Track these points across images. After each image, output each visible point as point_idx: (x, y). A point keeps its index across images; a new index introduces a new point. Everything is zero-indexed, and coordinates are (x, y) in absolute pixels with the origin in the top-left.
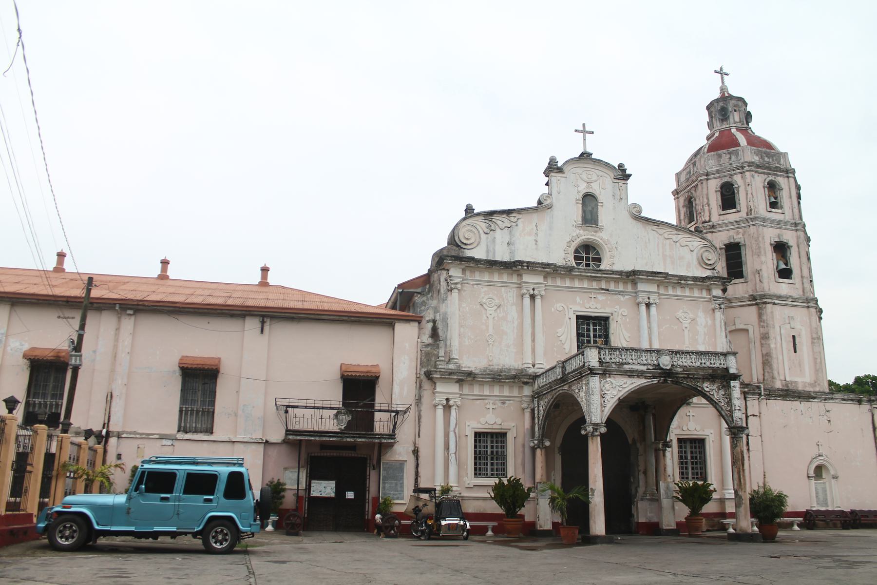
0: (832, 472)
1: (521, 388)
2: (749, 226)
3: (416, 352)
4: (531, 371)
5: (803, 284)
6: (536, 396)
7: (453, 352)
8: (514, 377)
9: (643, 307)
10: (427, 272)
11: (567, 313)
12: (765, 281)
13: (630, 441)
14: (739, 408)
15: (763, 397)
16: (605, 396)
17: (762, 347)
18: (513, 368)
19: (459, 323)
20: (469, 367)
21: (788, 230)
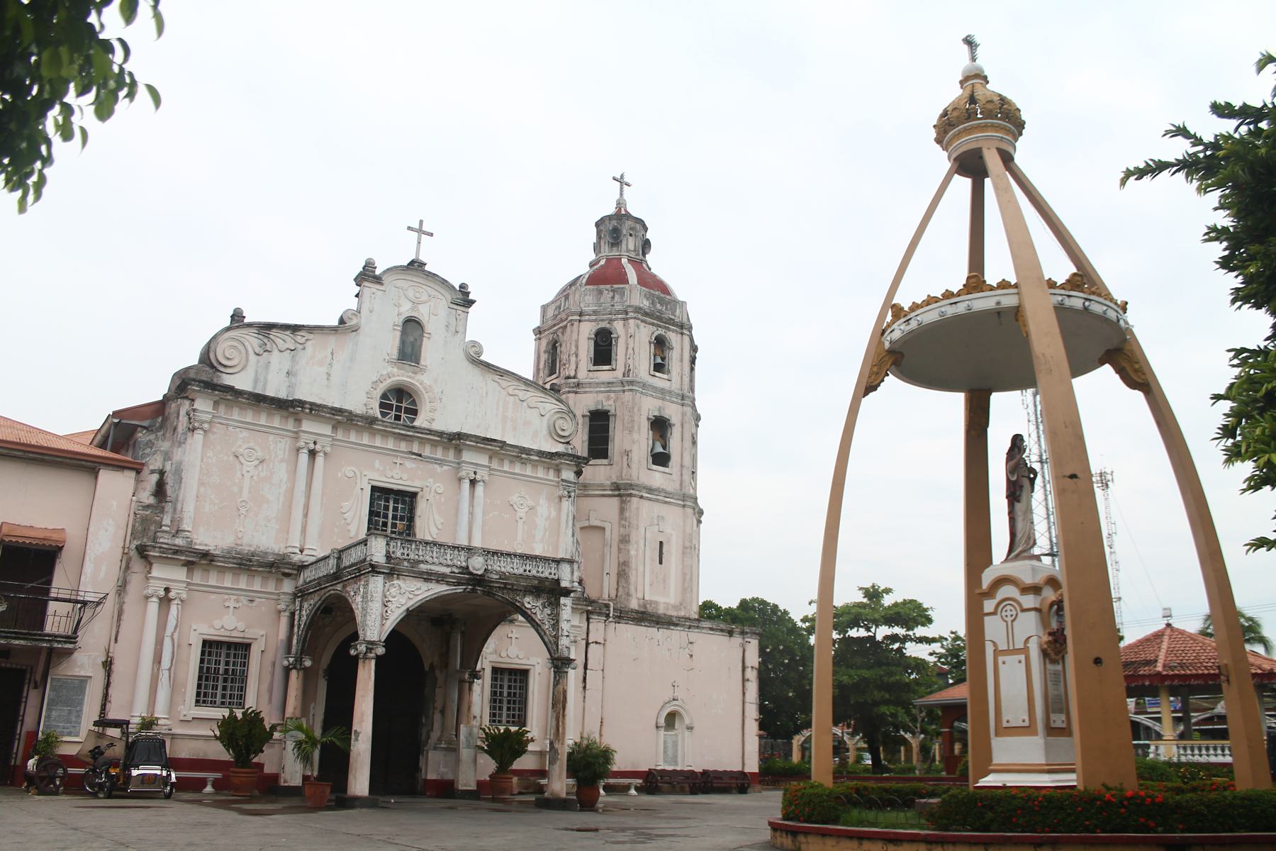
0: (687, 721)
1: (279, 581)
2: (624, 391)
3: (127, 515)
4: (297, 558)
5: (682, 475)
6: (299, 595)
7: (185, 521)
8: (271, 565)
9: (466, 484)
10: (162, 398)
11: (359, 482)
12: (634, 466)
13: (427, 668)
14: (567, 634)
15: (611, 619)
16: (389, 604)
17: (619, 553)
18: (272, 551)
19: (200, 479)
20: (206, 545)
21: (673, 402)
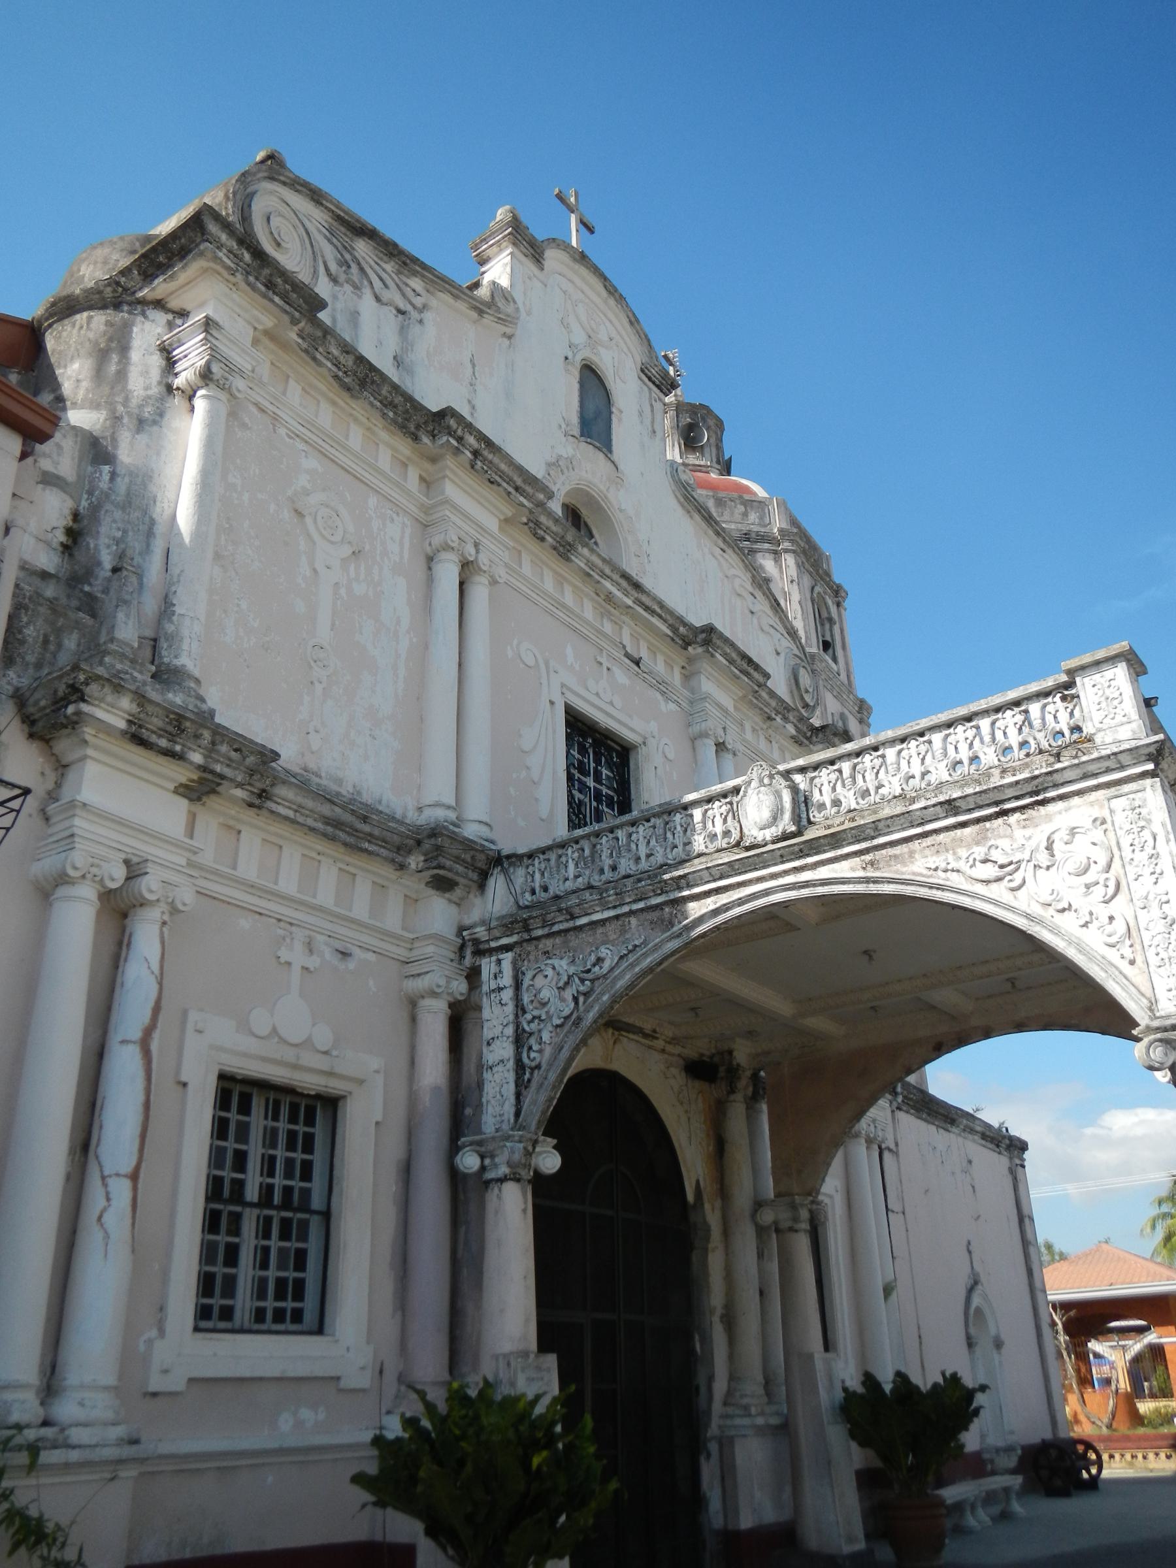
7: (185, 646)
